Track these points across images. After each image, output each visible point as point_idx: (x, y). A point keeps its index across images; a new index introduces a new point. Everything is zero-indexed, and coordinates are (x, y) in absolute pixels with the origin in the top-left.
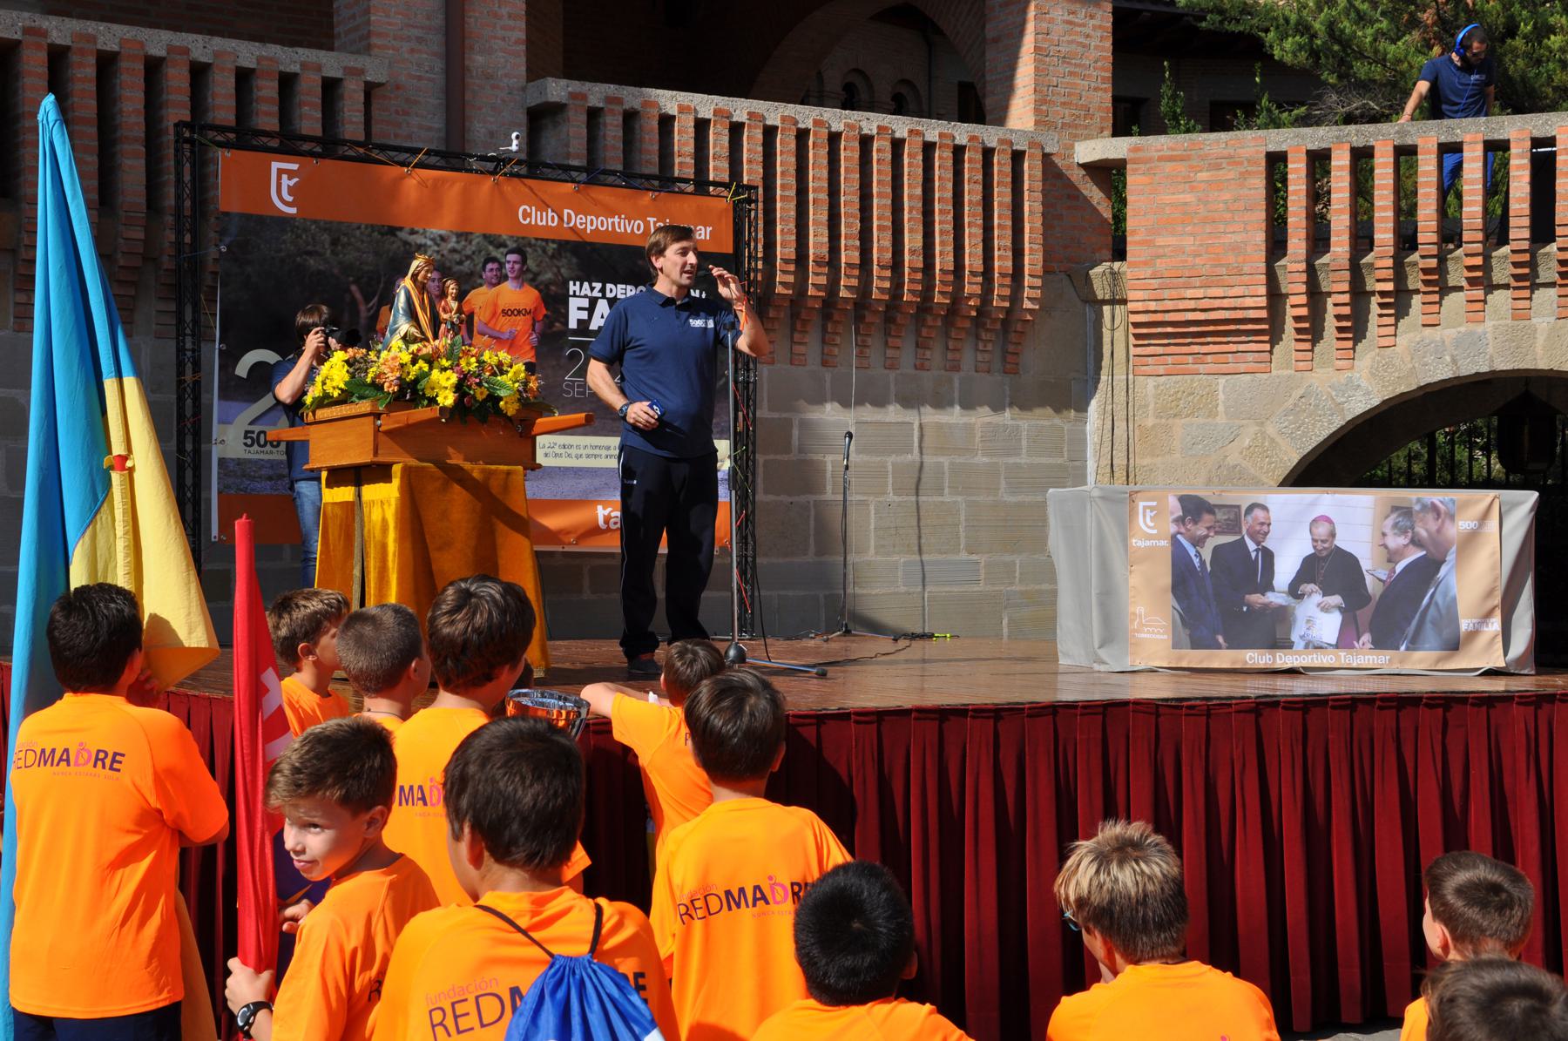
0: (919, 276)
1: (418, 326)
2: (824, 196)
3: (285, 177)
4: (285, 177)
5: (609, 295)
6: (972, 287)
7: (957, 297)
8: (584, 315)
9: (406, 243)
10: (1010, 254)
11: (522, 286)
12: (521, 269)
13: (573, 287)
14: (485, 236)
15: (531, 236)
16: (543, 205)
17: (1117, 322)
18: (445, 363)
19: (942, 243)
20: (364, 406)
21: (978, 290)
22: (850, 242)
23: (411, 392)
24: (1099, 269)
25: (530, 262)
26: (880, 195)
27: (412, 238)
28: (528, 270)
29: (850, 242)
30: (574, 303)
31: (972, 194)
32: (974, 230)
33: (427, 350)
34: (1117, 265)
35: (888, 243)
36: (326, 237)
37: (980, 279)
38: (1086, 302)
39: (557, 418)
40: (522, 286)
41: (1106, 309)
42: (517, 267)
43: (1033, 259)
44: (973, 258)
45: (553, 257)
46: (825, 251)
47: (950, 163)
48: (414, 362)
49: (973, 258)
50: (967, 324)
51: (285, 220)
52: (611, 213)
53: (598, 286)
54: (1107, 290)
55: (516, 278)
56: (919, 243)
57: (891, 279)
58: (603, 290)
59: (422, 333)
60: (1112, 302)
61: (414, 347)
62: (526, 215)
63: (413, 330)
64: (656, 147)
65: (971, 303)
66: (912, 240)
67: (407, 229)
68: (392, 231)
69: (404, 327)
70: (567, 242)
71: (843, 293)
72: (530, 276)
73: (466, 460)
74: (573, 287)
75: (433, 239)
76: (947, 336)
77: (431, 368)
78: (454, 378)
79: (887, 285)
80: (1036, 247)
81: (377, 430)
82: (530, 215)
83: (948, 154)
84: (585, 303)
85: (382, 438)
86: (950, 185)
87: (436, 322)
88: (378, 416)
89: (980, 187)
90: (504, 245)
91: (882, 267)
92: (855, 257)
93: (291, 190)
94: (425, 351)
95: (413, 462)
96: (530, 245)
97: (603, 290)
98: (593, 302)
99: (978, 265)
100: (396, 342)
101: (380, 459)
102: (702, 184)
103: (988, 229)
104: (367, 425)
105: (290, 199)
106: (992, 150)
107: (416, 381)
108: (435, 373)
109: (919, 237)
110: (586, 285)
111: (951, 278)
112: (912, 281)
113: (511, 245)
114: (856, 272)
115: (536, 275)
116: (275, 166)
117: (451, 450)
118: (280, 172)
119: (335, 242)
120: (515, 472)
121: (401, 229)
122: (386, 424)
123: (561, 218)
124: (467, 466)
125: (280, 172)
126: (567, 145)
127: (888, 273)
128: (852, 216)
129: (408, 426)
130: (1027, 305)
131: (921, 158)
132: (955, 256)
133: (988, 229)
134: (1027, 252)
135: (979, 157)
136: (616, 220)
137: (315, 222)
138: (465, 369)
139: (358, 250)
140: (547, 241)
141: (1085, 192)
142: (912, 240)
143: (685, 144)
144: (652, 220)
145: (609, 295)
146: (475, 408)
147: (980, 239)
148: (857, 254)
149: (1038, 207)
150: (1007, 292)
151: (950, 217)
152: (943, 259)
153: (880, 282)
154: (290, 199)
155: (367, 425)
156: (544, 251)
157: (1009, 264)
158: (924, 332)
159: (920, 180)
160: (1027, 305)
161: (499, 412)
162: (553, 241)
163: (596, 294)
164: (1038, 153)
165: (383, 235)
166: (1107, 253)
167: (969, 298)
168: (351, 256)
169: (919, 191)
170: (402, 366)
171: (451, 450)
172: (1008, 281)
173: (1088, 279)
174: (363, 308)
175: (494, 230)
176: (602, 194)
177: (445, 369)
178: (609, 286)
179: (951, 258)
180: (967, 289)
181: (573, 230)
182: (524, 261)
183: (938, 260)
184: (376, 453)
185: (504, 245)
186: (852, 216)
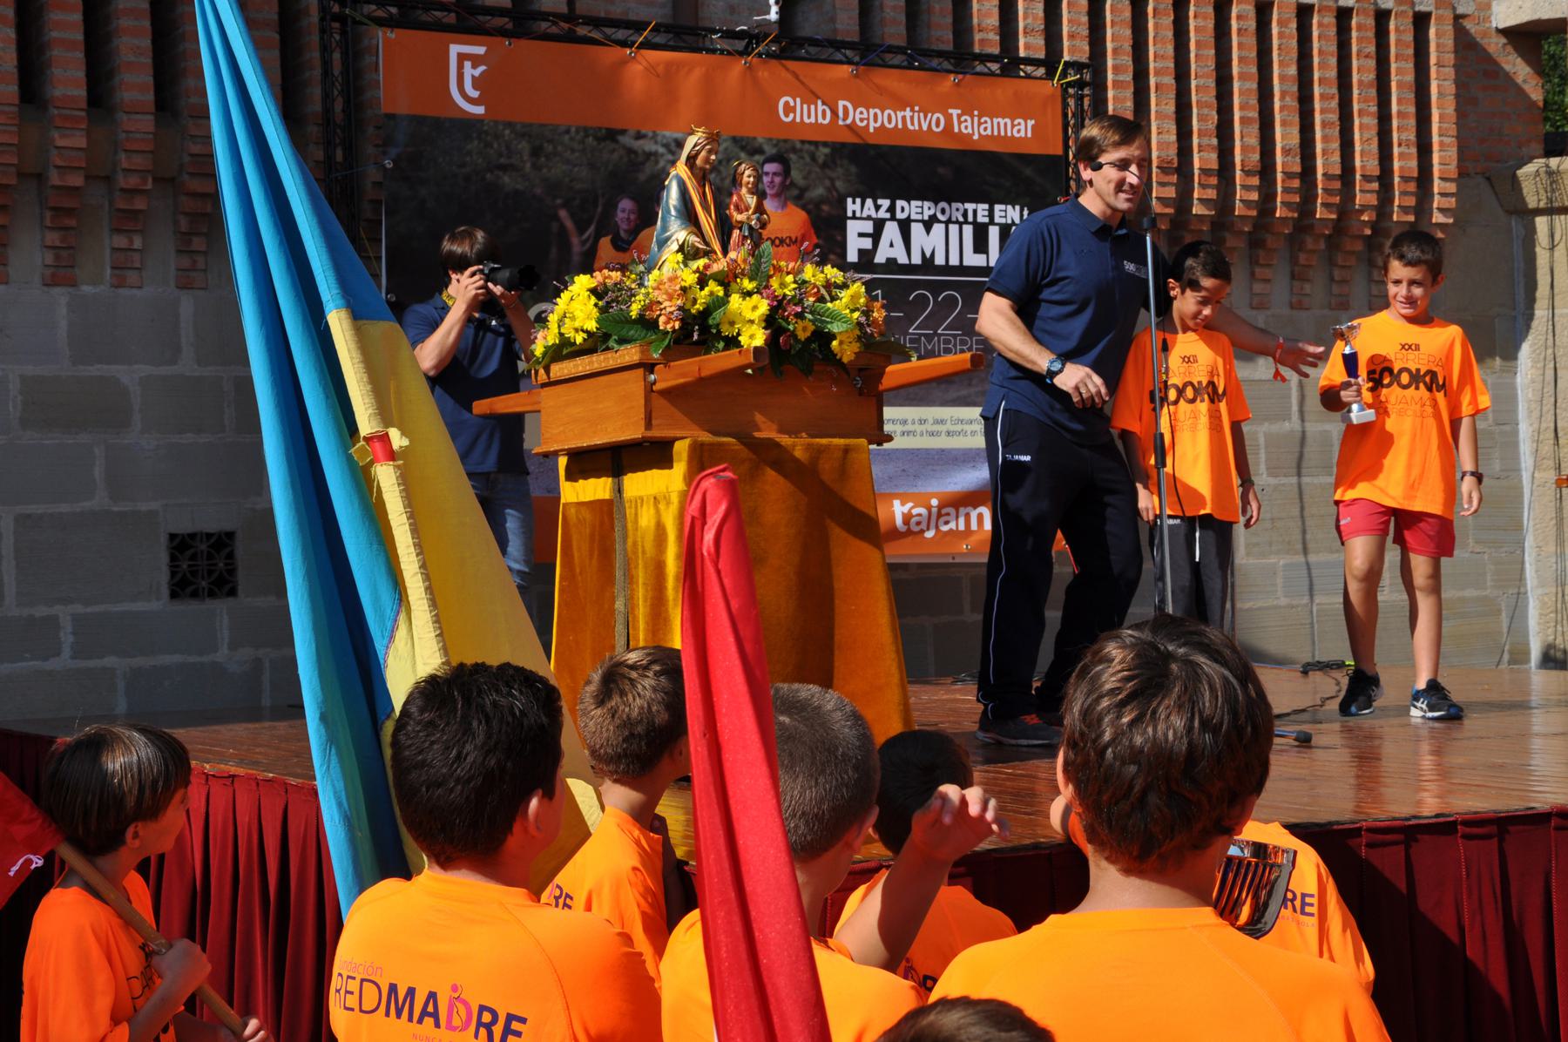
0: (1296, 183)
1: (699, 231)
2: (1169, 80)
3: (468, 64)
4: (468, 64)
5: (900, 215)
6: (1364, 196)
7: (1345, 209)
8: (867, 243)
9: (630, 151)
10: (1414, 150)
11: (784, 206)
12: (783, 183)
13: (852, 206)
14: (735, 140)
15: (796, 137)
16: (811, 97)
17: (1557, 238)
18: (748, 285)
19: (1325, 139)
20: (630, 354)
21: (1373, 200)
22: (1205, 141)
23: (700, 330)
24: (1530, 168)
25: (795, 174)
26: (1242, 77)
27: (637, 145)
28: (793, 184)
29: (1205, 141)
30: (853, 228)
31: (1362, 72)
32: (1366, 120)
33: (720, 265)
34: (1554, 162)
35: (1254, 141)
36: (524, 146)
37: (1375, 185)
38: (1510, 213)
39: (914, 367)
40: (784, 206)
41: (1541, 222)
42: (778, 180)
43: (1443, 157)
44: (1365, 159)
45: (825, 166)
46: (1172, 153)
47: (1333, 31)
48: (702, 282)
49: (1365, 159)
50: (1359, 246)
51: (470, 123)
52: (901, 104)
53: (885, 203)
54: (1543, 197)
55: (777, 195)
56: (1295, 139)
57: (1259, 189)
58: (892, 209)
59: (707, 244)
60: (1550, 211)
61: (701, 263)
62: (789, 109)
63: (693, 239)
64: (949, 20)
65: (1365, 218)
66: (1285, 136)
67: (632, 132)
68: (612, 135)
69: (680, 234)
70: (843, 145)
71: (1197, 209)
72: (795, 192)
73: (781, 431)
74: (852, 206)
75: (666, 146)
76: (1331, 263)
77: (727, 295)
78: (764, 307)
79: (1255, 196)
80: (1447, 140)
81: (649, 389)
82: (793, 110)
83: (1330, 20)
84: (868, 227)
85: (659, 403)
86: (1333, 61)
87: (725, 227)
88: (649, 367)
89: (1372, 63)
90: (760, 151)
91: (1247, 173)
92: (1212, 160)
93: (476, 83)
94: (716, 268)
95: (706, 437)
96: (794, 150)
97: (892, 209)
98: (879, 225)
99: (1373, 167)
100: (670, 257)
101: (656, 433)
102: (1010, 63)
103: (1384, 118)
104: (634, 384)
105: (475, 94)
106: (1387, 13)
107: (706, 312)
108: (735, 300)
109: (1295, 132)
110: (869, 202)
111: (1337, 185)
112: (1286, 190)
113: (770, 150)
114: (1214, 181)
115: (803, 191)
116: (455, 50)
117: (759, 418)
118: (462, 58)
119: (536, 152)
120: (857, 449)
121: (623, 132)
122: (664, 379)
123: (835, 113)
124: (785, 440)
125: (462, 58)
126: (833, 20)
127: (1255, 181)
128: (1207, 105)
129: (701, 381)
130: (1438, 218)
131: (1294, 25)
132: (1342, 157)
133: (1384, 118)
134: (1436, 147)
135: (1371, 22)
136: (908, 113)
137: (509, 125)
138: (779, 292)
139: (568, 162)
140: (816, 144)
141: (1507, 67)
142: (1285, 136)
143: (988, 15)
144: (955, 112)
145: (900, 215)
146: (795, 352)
147: (1374, 132)
148: (1214, 156)
149: (1450, 87)
150: (1411, 201)
151: (1334, 104)
152: (1326, 161)
153: (1245, 193)
154: (475, 94)
155: (634, 384)
156: (813, 158)
157: (1414, 164)
158: (1302, 258)
159: (1295, 55)
160: (1438, 218)
161: (831, 358)
162: (825, 144)
163: (883, 214)
164: (1449, 14)
165: (599, 139)
166: (1538, 147)
167: (1361, 212)
168: (557, 170)
169: (1293, 70)
170: (684, 290)
171: (759, 418)
172: (1412, 187)
173: (1515, 183)
174: (575, 241)
175: (745, 131)
176: (891, 80)
177: (749, 294)
178: (900, 203)
179: (1336, 158)
180: (1359, 199)
181: (852, 128)
182: (786, 172)
183: (1319, 162)
184: (649, 424)
185: (760, 151)
186: (1207, 105)
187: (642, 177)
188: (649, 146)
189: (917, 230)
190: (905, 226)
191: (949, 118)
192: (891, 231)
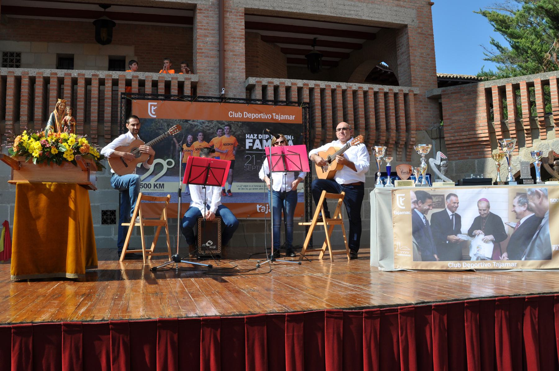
5: (259, 138)
8: (251, 145)
9: (191, 124)
25: (232, 129)
27: (193, 123)
30: (247, 141)
36: (165, 124)
45: (240, 127)
51: (152, 120)
53: (256, 135)
55: (228, 134)
58: (257, 137)
68: (187, 121)
70: (245, 122)
74: (247, 136)
75: (200, 123)
84: (252, 141)
90: (224, 124)
93: (154, 111)
96: (232, 123)
97: (257, 137)
98: (254, 140)
105: (154, 113)
110: (252, 135)
113: (226, 124)
116: (150, 104)
118: (151, 105)
121: (190, 120)
123: (243, 115)
125: (151, 105)
137: (162, 119)
144: (274, 114)
145: (259, 138)
154: (154, 113)
156: (237, 125)
163: (255, 138)
174: (177, 145)
178: (259, 135)
182: (230, 128)
185: (224, 124)
187: (194, 130)
188: (196, 123)
189: (264, 141)
190: (261, 141)
191: (272, 116)
192: (257, 142)
